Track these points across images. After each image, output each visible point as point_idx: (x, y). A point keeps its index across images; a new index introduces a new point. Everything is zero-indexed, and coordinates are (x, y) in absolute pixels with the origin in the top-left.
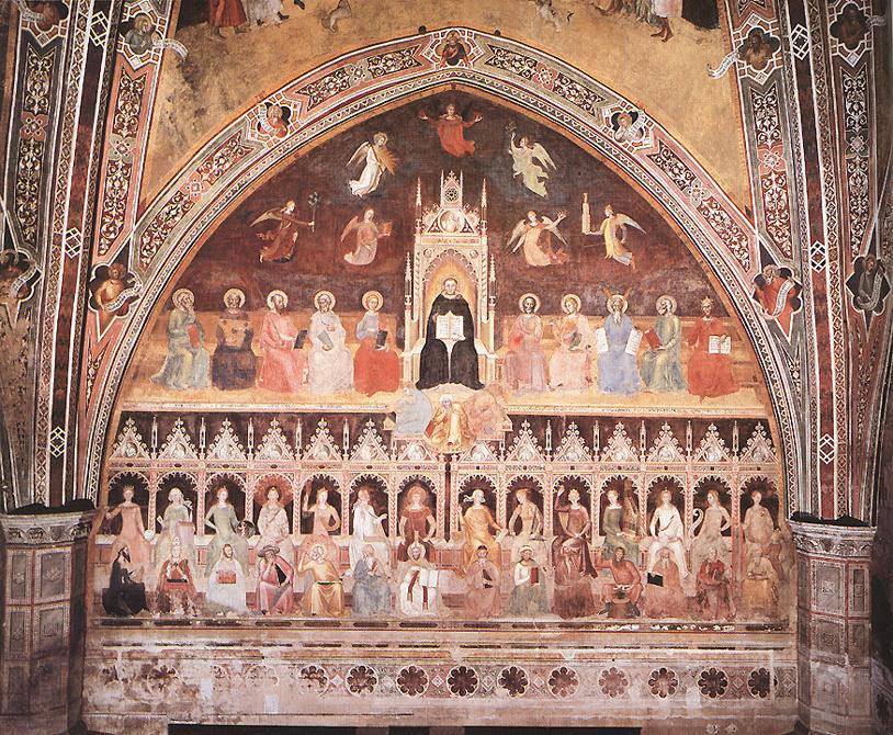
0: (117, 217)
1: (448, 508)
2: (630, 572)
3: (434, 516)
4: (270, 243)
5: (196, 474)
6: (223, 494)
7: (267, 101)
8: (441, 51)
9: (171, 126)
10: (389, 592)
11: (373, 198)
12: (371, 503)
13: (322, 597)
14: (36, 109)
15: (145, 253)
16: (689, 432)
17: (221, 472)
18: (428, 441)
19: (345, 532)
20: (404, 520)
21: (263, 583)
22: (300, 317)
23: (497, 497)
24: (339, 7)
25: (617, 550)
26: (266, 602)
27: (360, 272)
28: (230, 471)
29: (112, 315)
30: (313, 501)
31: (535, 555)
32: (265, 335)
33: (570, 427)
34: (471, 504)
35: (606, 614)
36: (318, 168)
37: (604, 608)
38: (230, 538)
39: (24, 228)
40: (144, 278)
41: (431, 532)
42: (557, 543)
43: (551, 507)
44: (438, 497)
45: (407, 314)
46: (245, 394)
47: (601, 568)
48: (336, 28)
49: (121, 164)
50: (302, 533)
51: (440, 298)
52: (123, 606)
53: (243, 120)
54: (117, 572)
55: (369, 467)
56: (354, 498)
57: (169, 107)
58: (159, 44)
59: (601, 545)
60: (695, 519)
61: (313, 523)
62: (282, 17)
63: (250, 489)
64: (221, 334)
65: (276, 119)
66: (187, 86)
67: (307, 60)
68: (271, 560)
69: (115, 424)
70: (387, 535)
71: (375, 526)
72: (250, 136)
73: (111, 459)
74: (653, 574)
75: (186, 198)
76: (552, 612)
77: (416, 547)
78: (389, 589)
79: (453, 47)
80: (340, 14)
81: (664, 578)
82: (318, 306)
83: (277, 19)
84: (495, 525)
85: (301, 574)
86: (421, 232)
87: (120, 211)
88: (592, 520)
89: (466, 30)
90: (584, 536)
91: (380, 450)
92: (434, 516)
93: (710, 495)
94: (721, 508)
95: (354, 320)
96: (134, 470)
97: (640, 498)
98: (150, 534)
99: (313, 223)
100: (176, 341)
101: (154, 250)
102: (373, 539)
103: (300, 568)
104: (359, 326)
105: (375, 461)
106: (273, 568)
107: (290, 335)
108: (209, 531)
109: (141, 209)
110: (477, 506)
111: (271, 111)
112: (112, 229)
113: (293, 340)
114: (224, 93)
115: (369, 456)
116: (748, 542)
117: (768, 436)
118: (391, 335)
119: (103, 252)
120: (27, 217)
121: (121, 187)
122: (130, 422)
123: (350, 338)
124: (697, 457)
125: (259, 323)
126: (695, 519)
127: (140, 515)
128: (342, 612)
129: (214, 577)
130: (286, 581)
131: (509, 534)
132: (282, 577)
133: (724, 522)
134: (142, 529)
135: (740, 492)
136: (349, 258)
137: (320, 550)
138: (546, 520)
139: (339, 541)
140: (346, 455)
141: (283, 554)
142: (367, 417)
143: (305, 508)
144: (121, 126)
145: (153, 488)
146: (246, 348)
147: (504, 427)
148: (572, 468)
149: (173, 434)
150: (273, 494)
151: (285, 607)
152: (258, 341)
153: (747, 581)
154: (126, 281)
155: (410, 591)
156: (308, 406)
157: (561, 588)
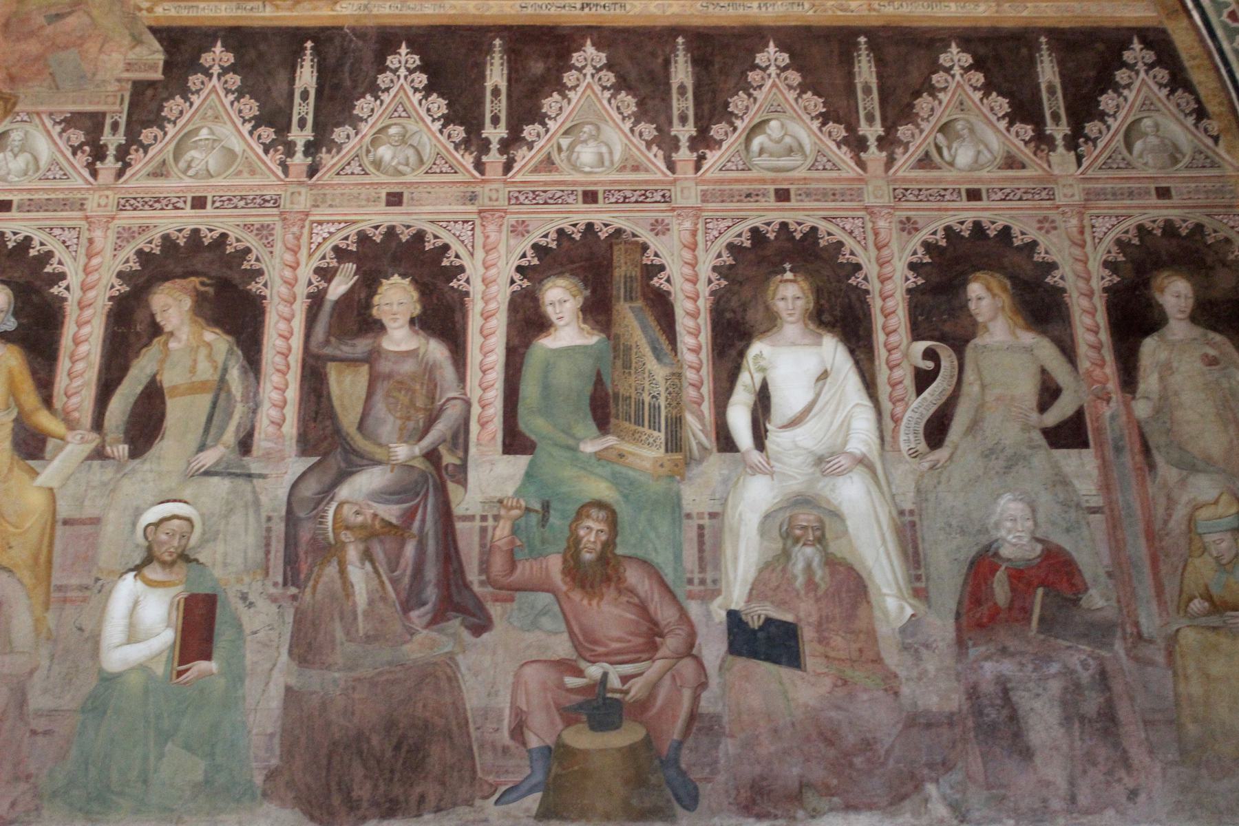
2: (643, 608)
16: (865, 71)
23: (71, 309)
25: (582, 512)
31: (209, 537)
33: (392, 61)
35: (533, 801)
37: (520, 770)
42: (310, 488)
43: (297, 343)
47: (510, 591)
59: (510, 490)
60: (923, 380)
74: (756, 615)
76: (265, 795)
81: (808, 634)
84: (45, 420)
88: (473, 391)
90: (432, 456)
93: (975, 289)
94: (1028, 338)
97: (681, 307)
116: (1167, 472)
117: (1179, 81)
124: (904, 161)
126: (923, 380)
131: (99, 454)
133: (1049, 393)
135: (1100, 279)
138: (269, 393)
147: (129, 66)
148: (395, 199)
153: (1190, 637)
157: (314, 680)
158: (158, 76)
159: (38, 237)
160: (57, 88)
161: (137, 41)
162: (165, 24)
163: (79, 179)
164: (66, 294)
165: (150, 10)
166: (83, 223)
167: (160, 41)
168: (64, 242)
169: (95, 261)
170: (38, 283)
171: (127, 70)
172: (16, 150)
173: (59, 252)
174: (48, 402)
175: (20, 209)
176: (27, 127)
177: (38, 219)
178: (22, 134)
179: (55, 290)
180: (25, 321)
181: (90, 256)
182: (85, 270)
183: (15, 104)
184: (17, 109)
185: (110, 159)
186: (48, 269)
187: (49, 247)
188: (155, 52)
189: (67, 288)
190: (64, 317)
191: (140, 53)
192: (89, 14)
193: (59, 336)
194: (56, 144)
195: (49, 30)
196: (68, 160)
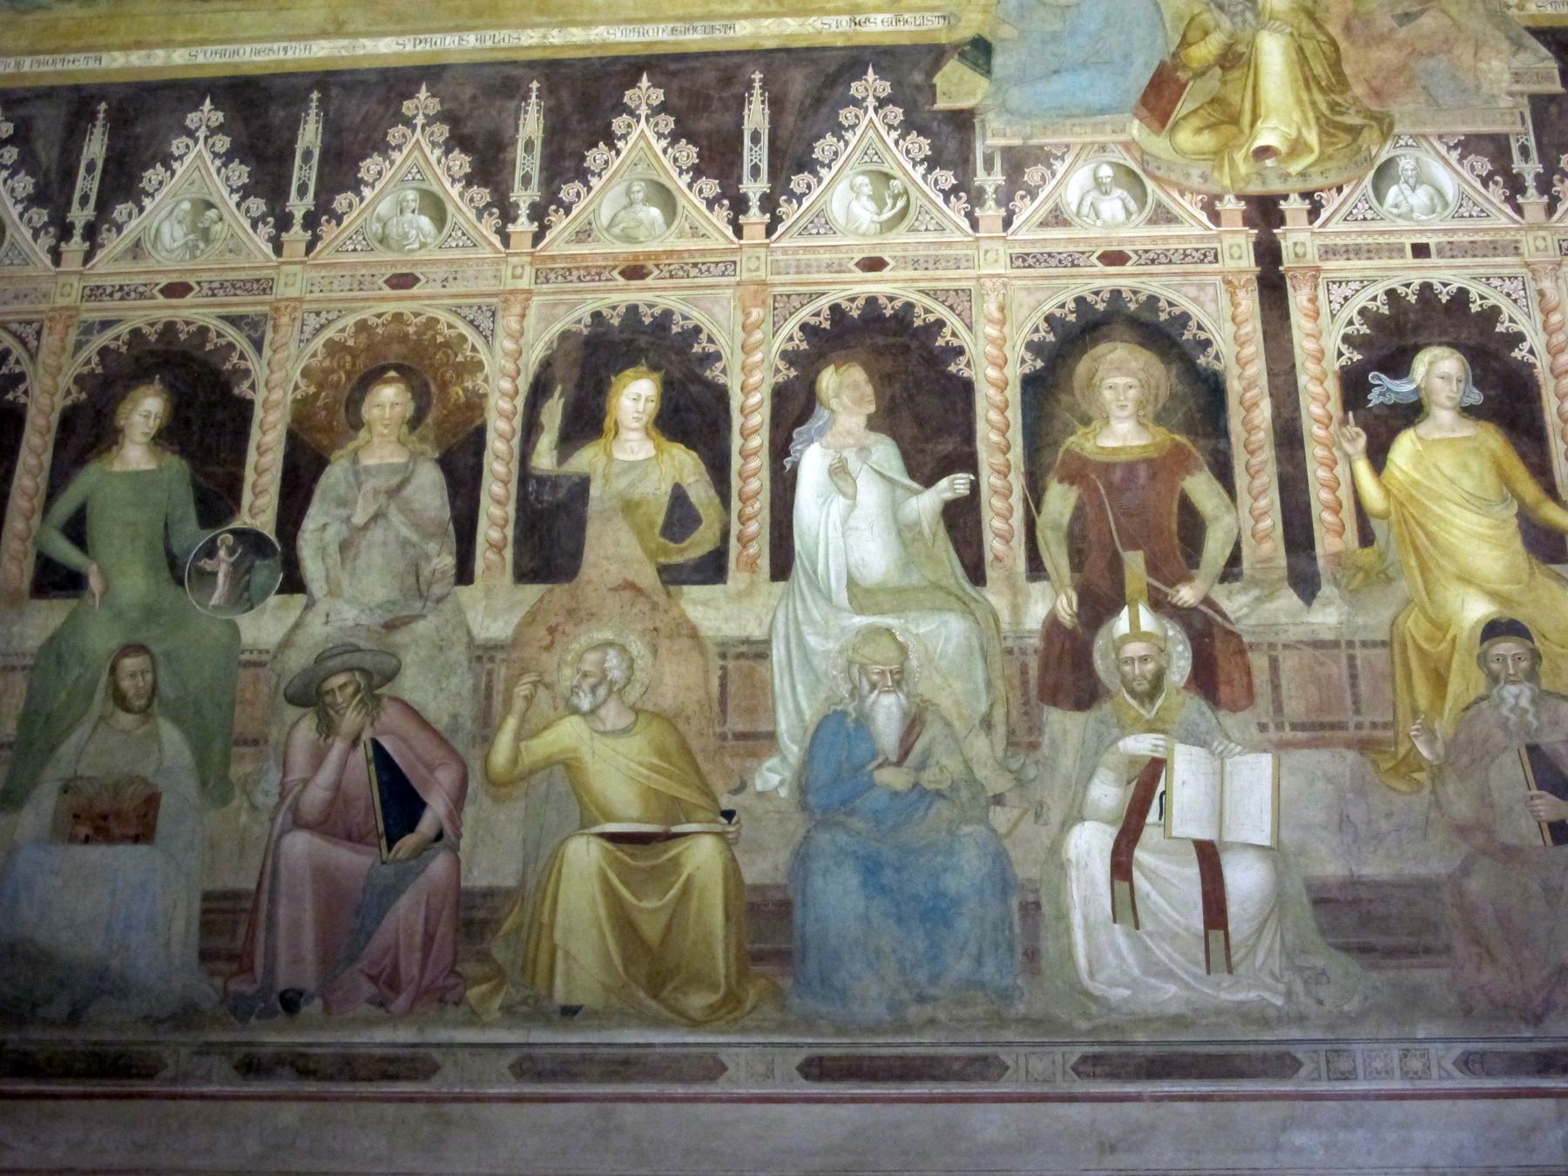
1: (1289, 438)
3: (1223, 472)
10: (1003, 880)
12: (885, 420)
13: (624, 923)
18: (1157, 144)
19: (752, 565)
20: (1060, 501)
21: (300, 845)
26: (308, 939)
28: (192, 312)
34: (1412, 412)
38: (151, 613)
41: (1215, 549)
44: (1234, 386)
50: (524, 575)
61: (580, 526)
68: (351, 719)
70: (976, 574)
71: (905, 534)
77: (1136, 634)
78: (1001, 859)
92: (1223, 472)
102: (894, 597)
105: (900, 236)
106: (361, 756)
110: (1443, 420)
115: (865, 214)
128: (732, 1000)
129: (44, 803)
130: (426, 826)
137: (613, 659)
140: (755, 217)
141: (414, 685)
142: (854, 61)
143: (544, 458)
150: (389, 399)
151: (410, 968)
155: (1121, 867)
156: (577, 35)
158: (1556, 87)
159: (1475, 290)
160: (1436, 102)
161: (1518, 46)
162: (1546, 24)
163: (1501, 218)
164: (1532, 359)
165: (1521, 7)
166: (1524, 270)
167: (1547, 44)
168: (1509, 295)
169: (1555, 318)
170: (1492, 346)
171: (1517, 82)
172: (1411, 181)
173: (1507, 308)
174: (1551, 491)
175: (1440, 253)
176: (1418, 154)
177: (1467, 267)
178: (1413, 162)
179: (1517, 354)
180: (1492, 392)
181: (1547, 313)
182: (1545, 329)
183: (1391, 125)
184: (1396, 130)
185: (1532, 191)
186: (1500, 328)
187: (1491, 302)
188: (1544, 59)
189: (1531, 351)
190: (1539, 387)
191: (1524, 60)
192: (1445, 12)
193: (1541, 410)
194: (1459, 174)
195: (1402, 33)
196: (1480, 193)
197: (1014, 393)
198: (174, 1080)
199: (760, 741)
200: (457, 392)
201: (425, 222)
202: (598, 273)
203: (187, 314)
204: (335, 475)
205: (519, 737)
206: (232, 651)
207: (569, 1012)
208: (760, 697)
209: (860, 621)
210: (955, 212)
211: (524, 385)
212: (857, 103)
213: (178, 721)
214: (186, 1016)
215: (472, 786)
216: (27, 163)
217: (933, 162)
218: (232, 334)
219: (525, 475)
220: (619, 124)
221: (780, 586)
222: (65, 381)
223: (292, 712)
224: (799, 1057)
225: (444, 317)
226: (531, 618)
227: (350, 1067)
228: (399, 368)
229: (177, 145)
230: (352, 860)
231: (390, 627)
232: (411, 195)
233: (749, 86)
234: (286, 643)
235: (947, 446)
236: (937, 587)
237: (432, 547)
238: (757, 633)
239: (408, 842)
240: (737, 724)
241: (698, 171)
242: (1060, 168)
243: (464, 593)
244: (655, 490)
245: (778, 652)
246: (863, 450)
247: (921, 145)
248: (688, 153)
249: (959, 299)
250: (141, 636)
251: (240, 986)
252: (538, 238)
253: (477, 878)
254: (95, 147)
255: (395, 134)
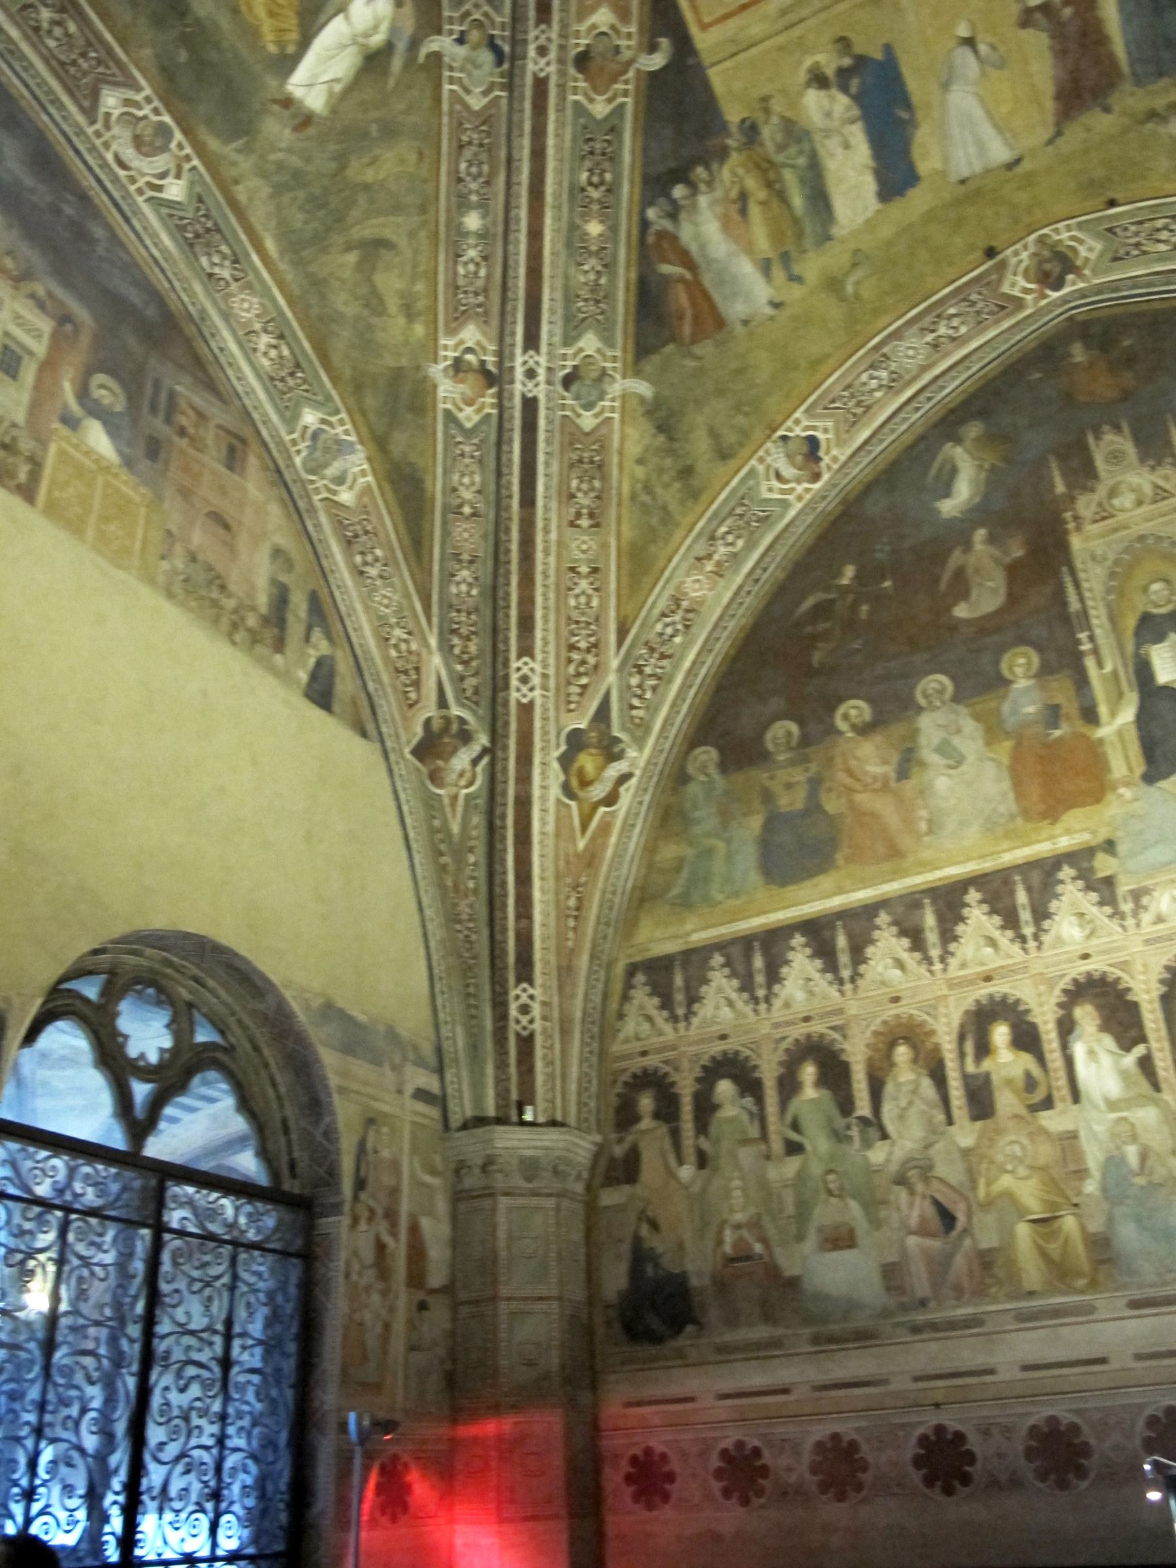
0: (588, 650)
4: (825, 636)
5: (755, 1046)
6: (809, 1072)
7: (780, 433)
8: (1032, 273)
9: (646, 498)
11: (978, 514)
12: (1105, 1027)
13: (1044, 1254)
14: (467, 510)
15: (636, 702)
17: (798, 1032)
21: (912, 1241)
22: (898, 730)
24: (855, 265)
27: (986, 627)
28: (817, 1028)
29: (595, 807)
30: (984, 1049)
32: (842, 777)
36: (875, 507)
38: (832, 1157)
39: (462, 678)
40: (640, 743)
45: (1090, 663)
46: (825, 882)
48: (857, 296)
49: (584, 569)
50: (975, 1117)
51: (1146, 620)
52: (655, 1322)
53: (752, 473)
54: (640, 1257)
55: (1086, 956)
56: (1066, 1027)
57: (640, 471)
58: (618, 386)
62: (776, 305)
63: (857, 1054)
64: (768, 797)
65: (799, 459)
66: (661, 438)
67: (827, 356)
68: (920, 1187)
69: (617, 987)
70: (1156, 1087)
71: (1124, 1075)
72: (769, 490)
73: (616, 1048)
75: (685, 604)
79: (1048, 261)
80: (858, 274)
82: (922, 702)
83: (769, 311)
85: (987, 1205)
86: (1078, 529)
87: (592, 639)
89: (1061, 225)
91: (1100, 915)
95: (992, 704)
96: (652, 1061)
98: (686, 1172)
99: (887, 584)
100: (697, 830)
101: (648, 695)
103: (982, 1192)
104: (1006, 708)
105: (1094, 941)
106: (927, 1202)
107: (885, 762)
108: (794, 1148)
109: (622, 632)
111: (792, 445)
112: (582, 669)
113: (889, 770)
114: (714, 434)
118: (1071, 707)
119: (572, 706)
120: (465, 663)
121: (588, 604)
122: (640, 978)
123: (993, 730)
125: (829, 762)
127: (667, 1143)
132: (947, 1218)
134: (672, 1160)
136: (961, 611)
139: (1054, 1121)
140: (1032, 944)
141: (941, 1170)
144: (578, 515)
145: (686, 1087)
146: (814, 807)
149: (707, 981)
150: (902, 1052)
152: (830, 790)
154: (611, 752)
197: (1157, 1005)
198: (887, 1338)
199: (1081, 1173)
200: (929, 1045)
201: (898, 972)
202: (970, 982)
203: (814, 1029)
204: (889, 1088)
205: (988, 1184)
206: (871, 1171)
207: (1031, 1294)
208: (1079, 1156)
209: (1113, 1116)
210: (1114, 925)
211: (954, 1035)
212: (1062, 882)
213: (854, 1197)
214: (885, 1313)
215: (975, 1207)
216: (734, 974)
217: (1101, 903)
218: (836, 1036)
219: (966, 1077)
220: (965, 911)
221: (1075, 1107)
222: (774, 1065)
223: (897, 1188)
224: (1124, 1301)
225: (915, 1012)
226: (980, 1137)
227: (952, 1325)
228: (904, 1038)
229: (790, 955)
230: (935, 1244)
231: (927, 1147)
232: (889, 961)
233: (1014, 883)
234: (888, 1161)
235: (1133, 1033)
236: (1142, 1096)
237: (935, 1112)
238: (1071, 1127)
239: (954, 1233)
240: (1072, 1167)
241: (1003, 927)
242: (1156, 894)
243: (953, 1129)
244: (1017, 1072)
245: (1082, 1134)
246: (1099, 1041)
247: (1094, 896)
248: (997, 920)
249: (1124, 965)
250: (832, 1166)
251: (904, 1299)
252: (945, 970)
253: (984, 1244)
254: (758, 962)
255: (876, 934)
